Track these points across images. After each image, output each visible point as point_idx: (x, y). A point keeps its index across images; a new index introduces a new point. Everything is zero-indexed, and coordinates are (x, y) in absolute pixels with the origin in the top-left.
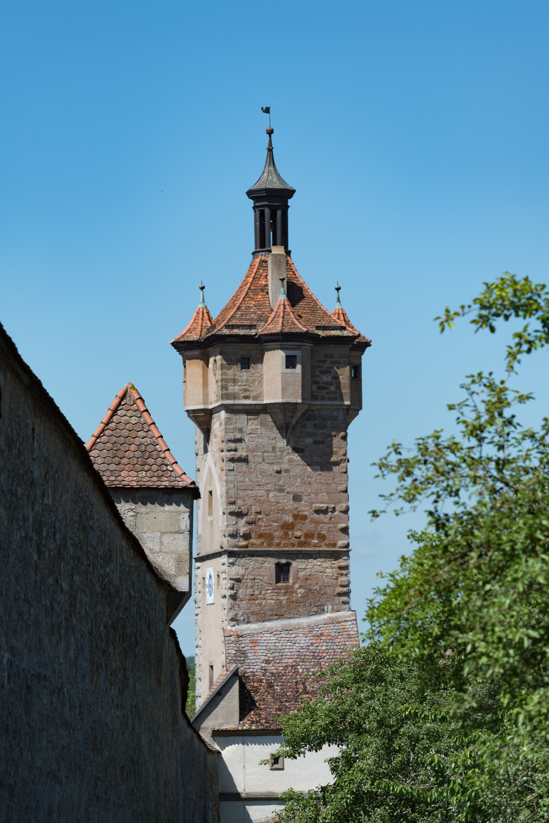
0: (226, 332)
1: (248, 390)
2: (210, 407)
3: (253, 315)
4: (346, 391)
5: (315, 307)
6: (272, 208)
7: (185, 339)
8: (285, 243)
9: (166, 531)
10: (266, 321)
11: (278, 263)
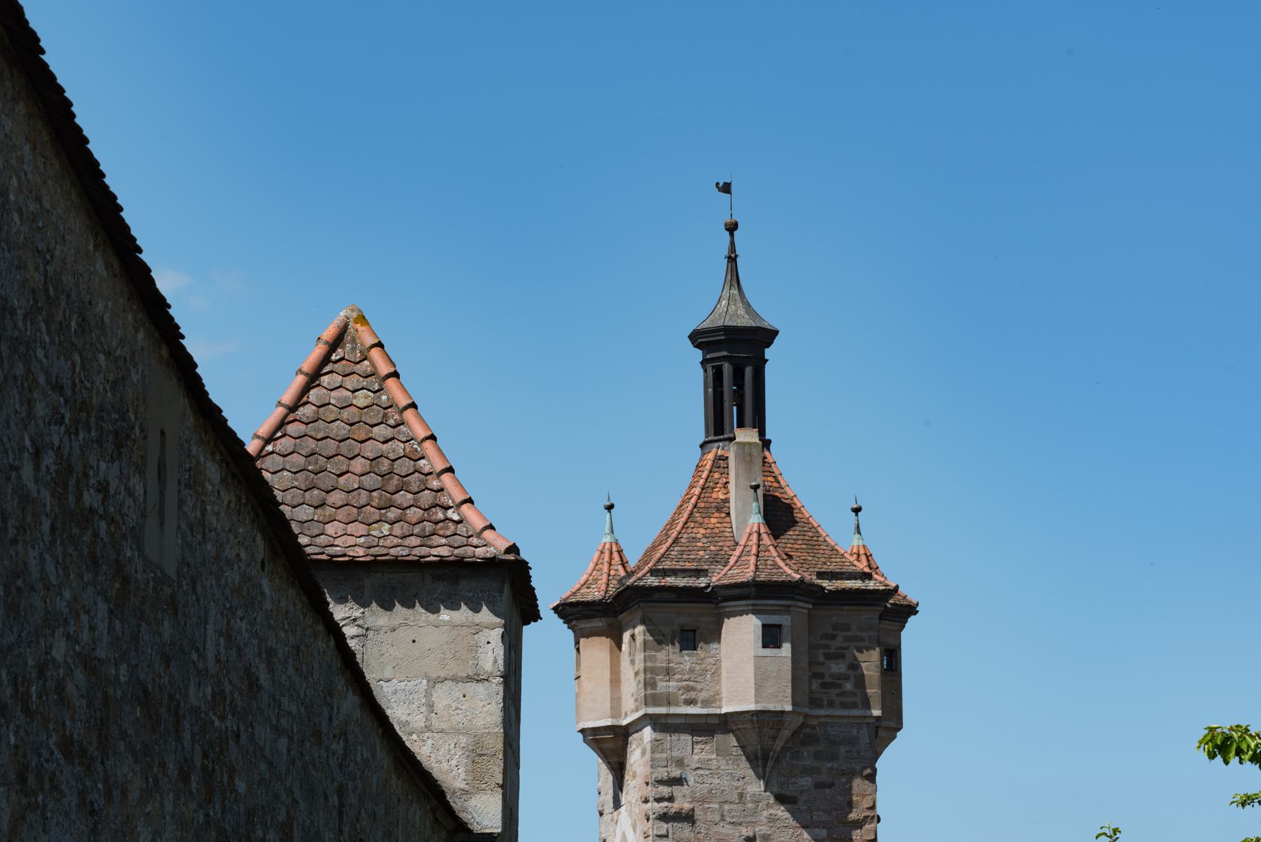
0: (653, 581)
1: (693, 689)
2: (625, 722)
3: (701, 553)
4: (873, 691)
5: (815, 540)
6: (735, 363)
7: (579, 598)
8: (759, 423)
9: (443, 675)
10: (727, 562)
11: (748, 458)
